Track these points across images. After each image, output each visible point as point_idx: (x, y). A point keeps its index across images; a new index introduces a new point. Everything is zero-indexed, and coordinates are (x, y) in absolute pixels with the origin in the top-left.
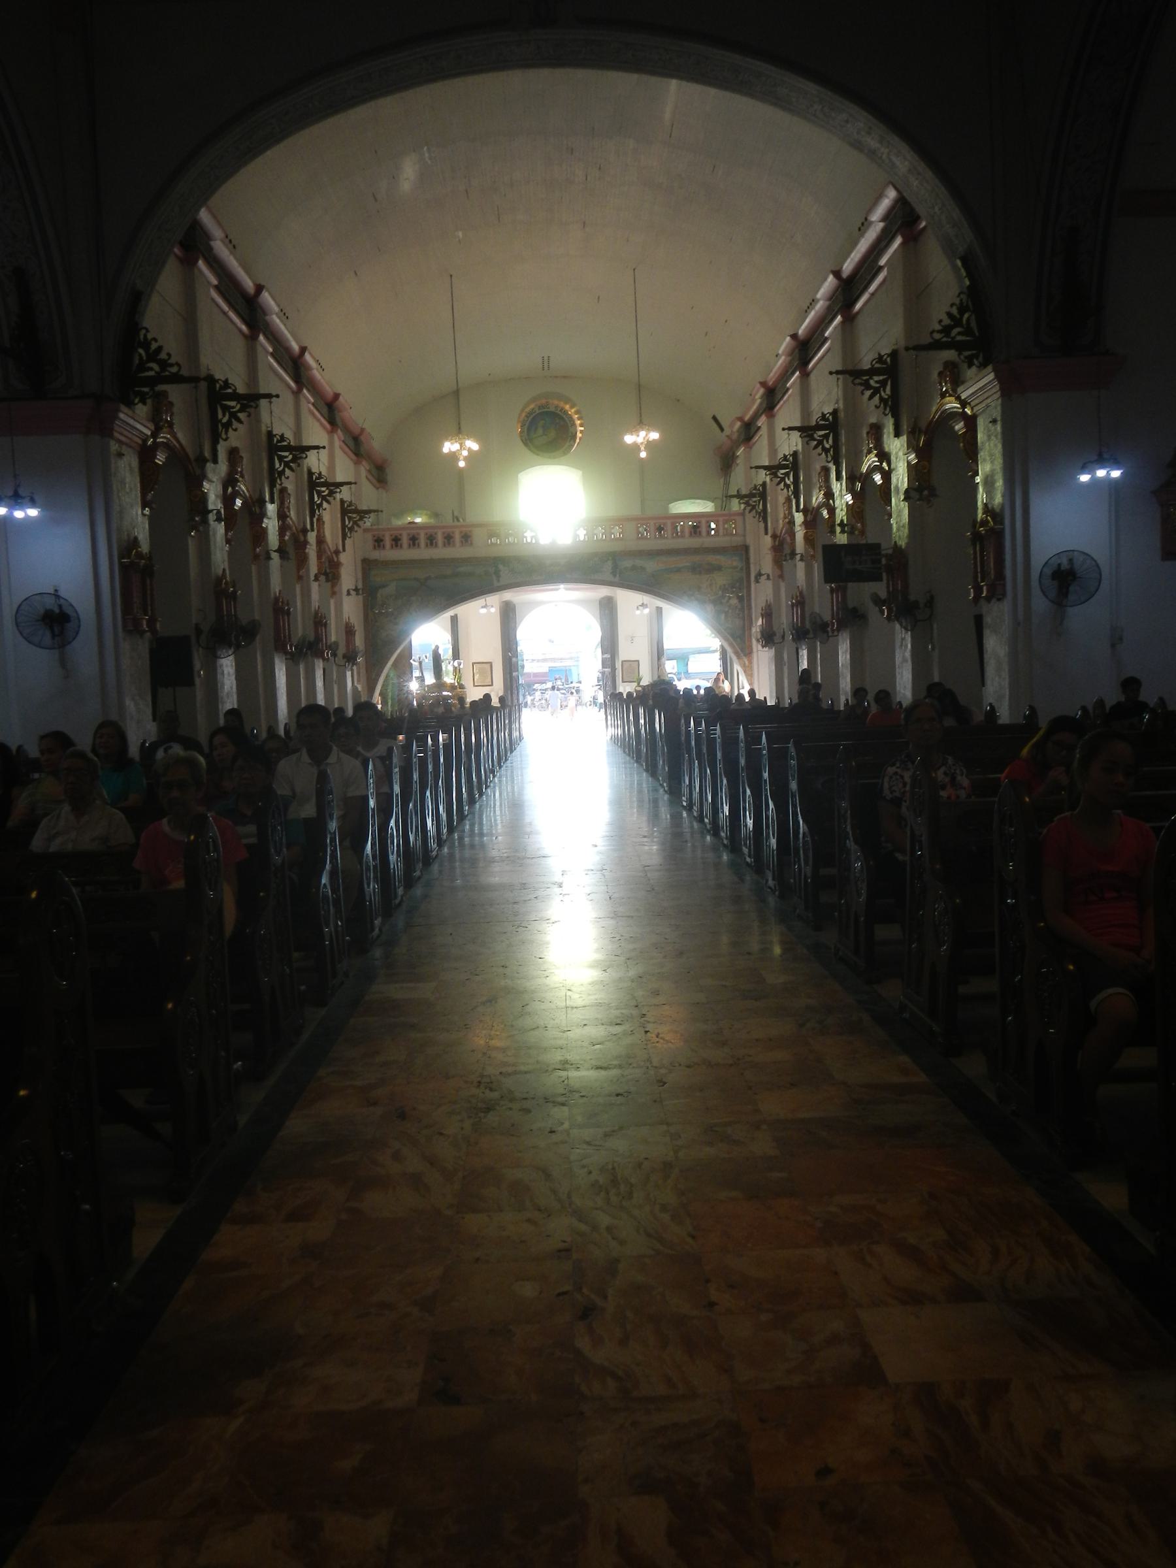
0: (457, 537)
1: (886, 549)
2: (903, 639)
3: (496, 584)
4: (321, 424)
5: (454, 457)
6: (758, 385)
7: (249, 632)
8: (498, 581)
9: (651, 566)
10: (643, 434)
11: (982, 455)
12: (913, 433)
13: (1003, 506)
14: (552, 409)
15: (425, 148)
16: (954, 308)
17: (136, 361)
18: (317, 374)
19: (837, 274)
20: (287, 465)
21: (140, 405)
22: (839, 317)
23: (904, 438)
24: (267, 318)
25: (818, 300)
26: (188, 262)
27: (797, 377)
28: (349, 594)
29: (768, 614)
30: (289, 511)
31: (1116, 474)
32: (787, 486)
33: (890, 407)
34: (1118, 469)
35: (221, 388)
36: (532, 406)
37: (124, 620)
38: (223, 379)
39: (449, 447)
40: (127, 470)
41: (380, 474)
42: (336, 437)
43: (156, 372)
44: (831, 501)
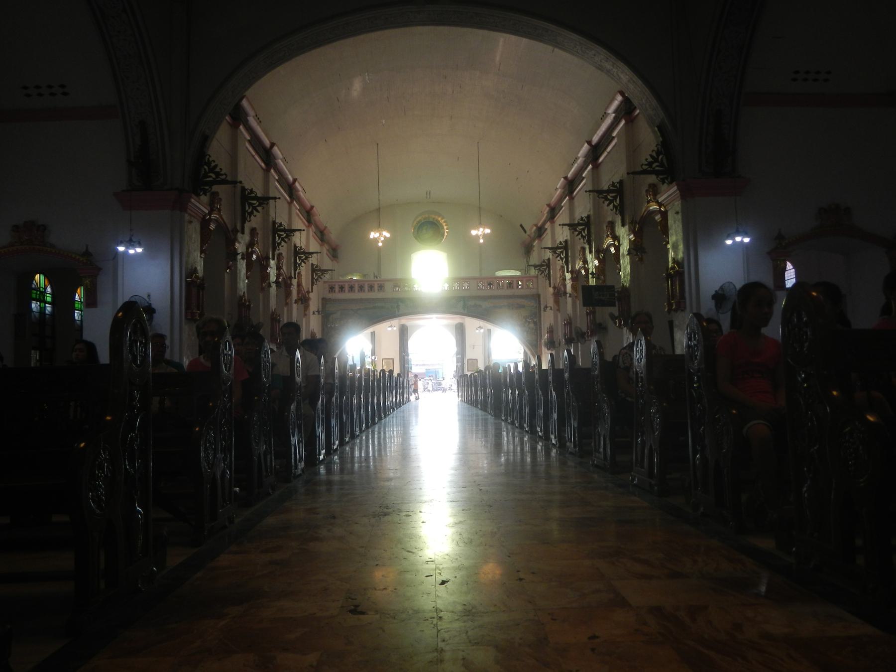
0: (376, 287)
1: (618, 287)
3: (397, 313)
4: (303, 222)
5: (376, 240)
8: (398, 311)
9: (485, 304)
10: (481, 229)
11: (670, 232)
12: (633, 223)
13: (683, 258)
14: (431, 220)
15: (366, 74)
18: (301, 194)
19: (589, 143)
21: (203, 195)
22: (591, 166)
23: (627, 227)
24: (276, 161)
25: (579, 158)
26: (235, 125)
27: (568, 200)
28: (314, 313)
29: (551, 331)
30: (283, 266)
31: (747, 240)
32: (562, 259)
34: (748, 237)
36: (420, 218)
37: (186, 313)
38: (250, 189)
39: (373, 235)
41: (334, 253)
42: (311, 229)
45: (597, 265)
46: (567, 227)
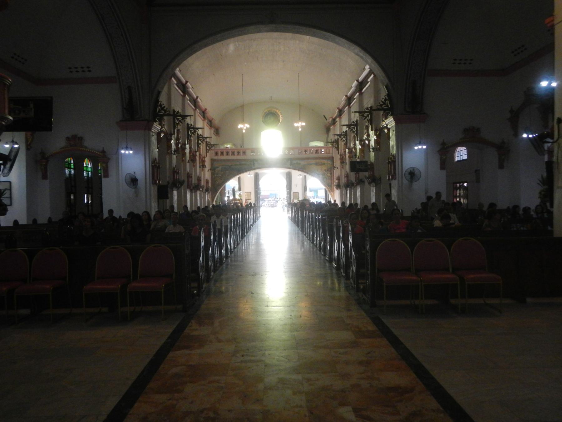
0: (241, 153)
1: (369, 163)
2: (373, 189)
3: (253, 167)
4: (201, 118)
5: (242, 129)
6: (336, 109)
7: (182, 183)
8: (254, 166)
9: (303, 163)
11: (391, 139)
12: (376, 131)
13: (396, 153)
14: (272, 112)
15: (237, 42)
16: (383, 99)
17: (158, 110)
18: (201, 104)
19: (358, 81)
23: (374, 131)
24: (188, 90)
25: (352, 87)
27: (347, 108)
28: (208, 171)
29: (338, 179)
31: (425, 147)
32: (344, 141)
36: (266, 111)
38: (177, 111)
39: (240, 126)
40: (154, 139)
41: (217, 131)
45: (360, 148)
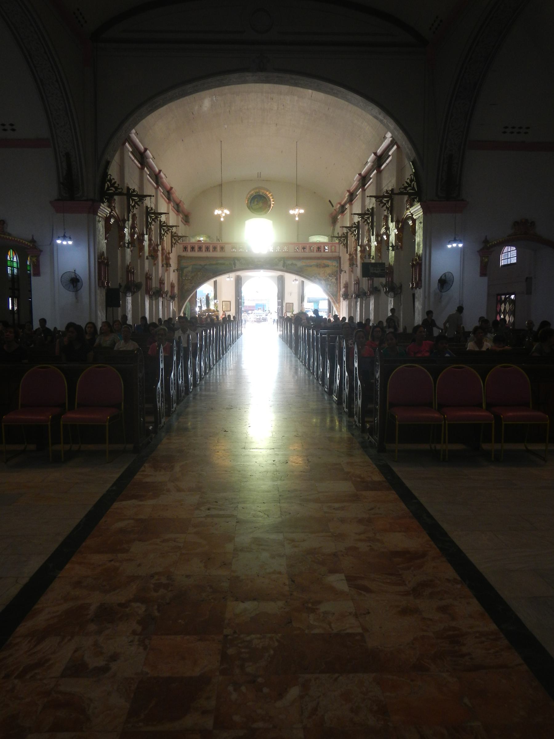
0: (218, 249)
1: (387, 266)
2: (391, 301)
3: (234, 268)
5: (219, 216)
6: (346, 191)
7: (138, 286)
8: (235, 267)
9: (300, 264)
10: (297, 210)
12: (397, 223)
13: (422, 254)
14: (261, 194)
15: (214, 96)
16: (409, 180)
17: (106, 187)
18: (165, 180)
19: (375, 154)
20: (153, 220)
22: (375, 171)
24: (147, 160)
27: (360, 191)
28: (174, 271)
29: (346, 286)
30: (152, 237)
31: (460, 245)
32: (355, 235)
33: (390, 211)
34: (461, 243)
35: (132, 192)
37: (98, 282)
38: (133, 189)
39: (217, 212)
40: (101, 226)
41: (186, 219)
42: (170, 205)
43: (113, 191)
44: (370, 243)
45: (376, 245)
46: (357, 215)
